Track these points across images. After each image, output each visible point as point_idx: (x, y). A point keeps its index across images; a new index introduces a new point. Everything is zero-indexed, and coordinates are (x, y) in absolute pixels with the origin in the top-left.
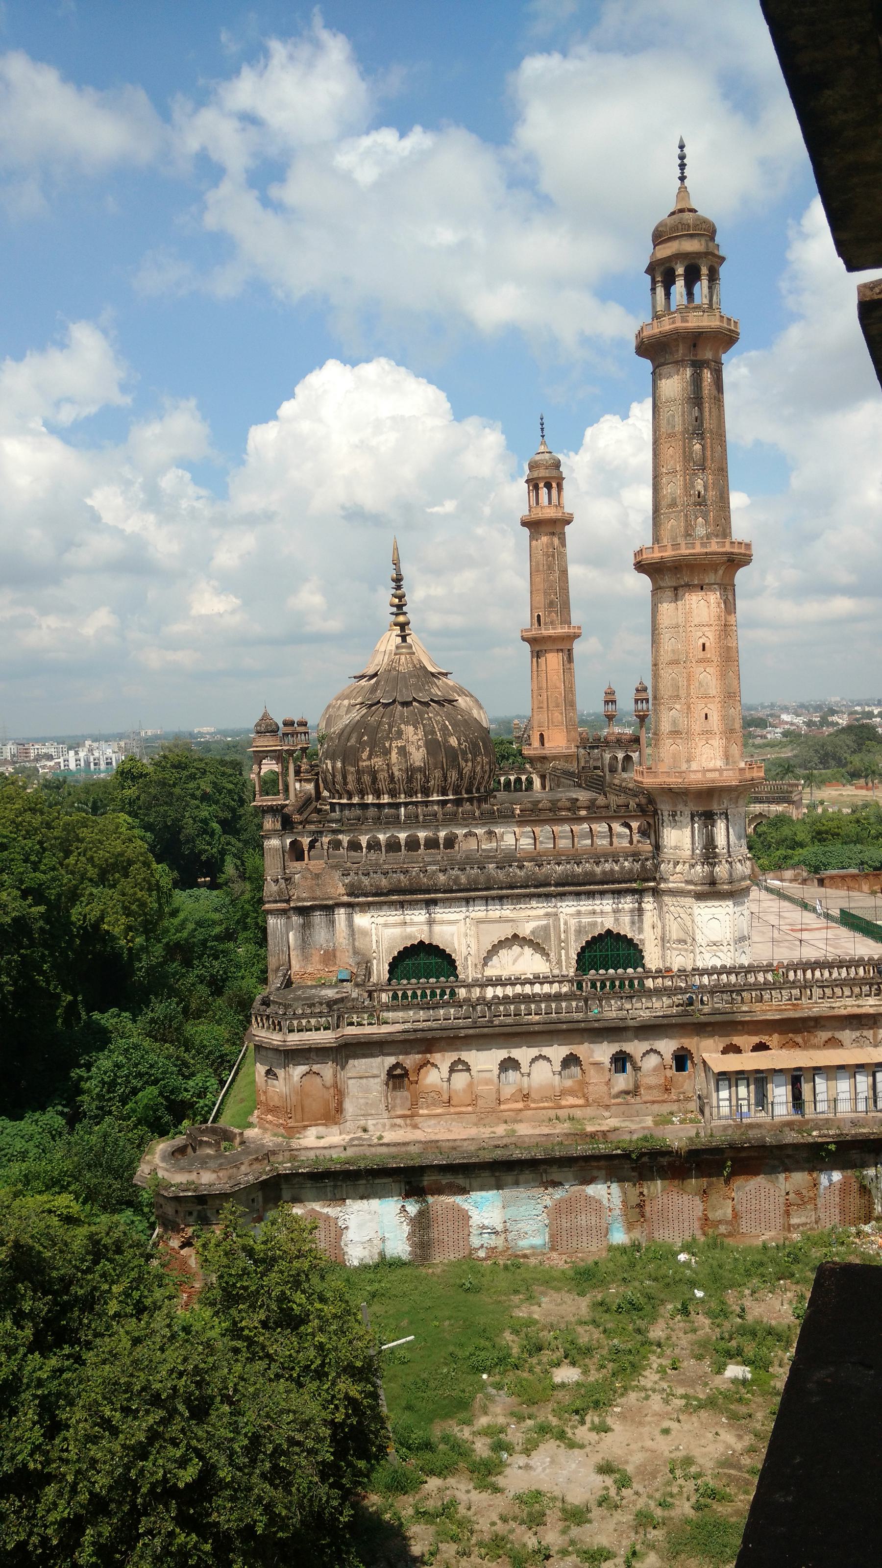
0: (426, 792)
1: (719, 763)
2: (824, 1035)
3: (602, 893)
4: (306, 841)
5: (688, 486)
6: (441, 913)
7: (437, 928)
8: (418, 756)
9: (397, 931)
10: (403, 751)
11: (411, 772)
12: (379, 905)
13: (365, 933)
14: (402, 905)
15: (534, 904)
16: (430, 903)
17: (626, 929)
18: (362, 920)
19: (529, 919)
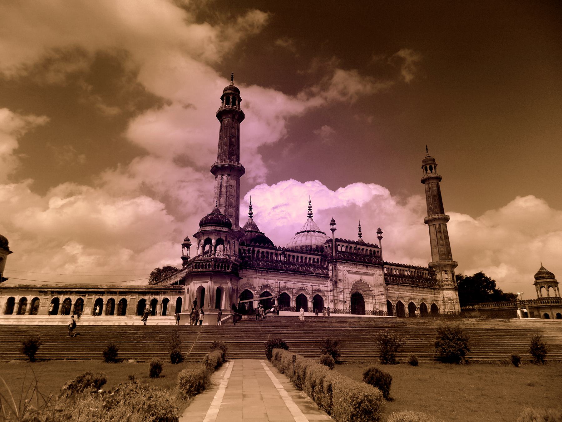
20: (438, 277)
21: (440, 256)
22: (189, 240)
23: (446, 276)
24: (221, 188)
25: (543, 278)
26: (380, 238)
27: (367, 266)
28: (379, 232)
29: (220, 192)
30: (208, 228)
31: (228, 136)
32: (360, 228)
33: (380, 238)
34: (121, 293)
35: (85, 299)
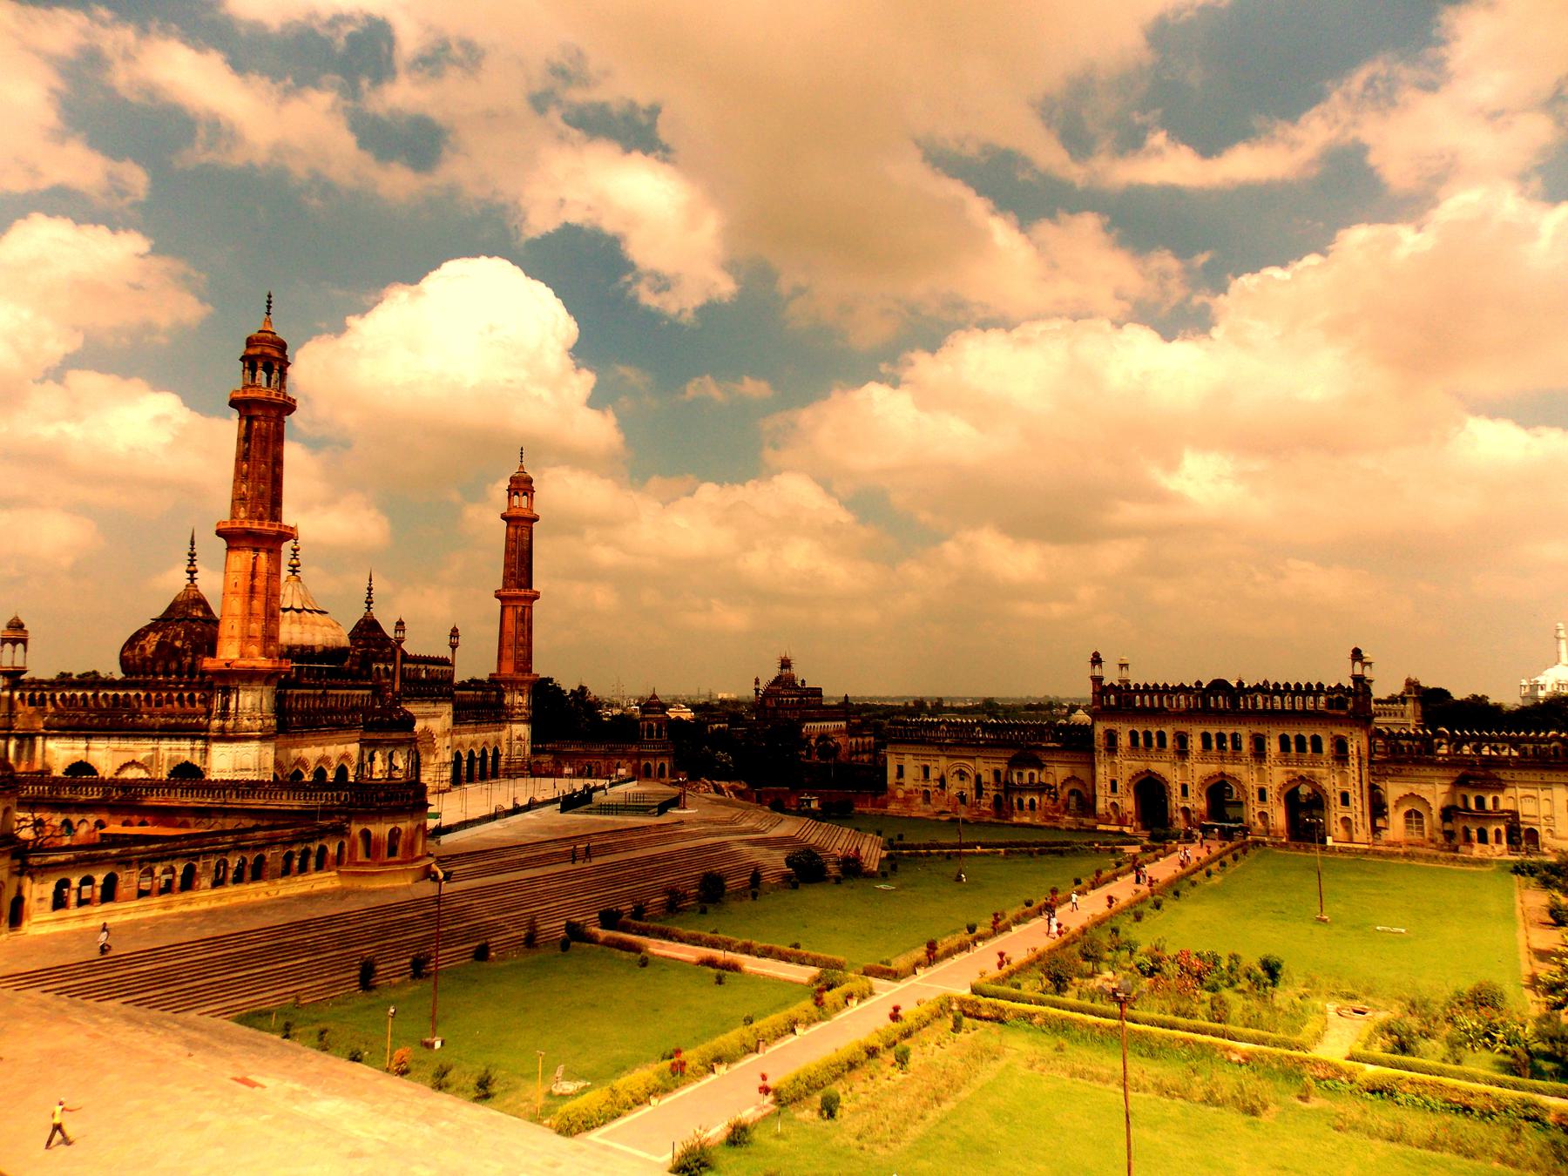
0: (156, 675)
1: (236, 656)
2: (179, 819)
3: (185, 737)
4: (27, 694)
5: (236, 488)
6: (95, 744)
7: (91, 753)
8: (150, 649)
9: (69, 753)
10: (143, 648)
11: (144, 659)
12: (59, 736)
13: (52, 753)
14: (73, 737)
15: (145, 741)
16: (88, 737)
17: (197, 762)
18: (51, 745)
19: (142, 750)
20: (508, 699)
21: (516, 664)
22: (20, 626)
23: (519, 699)
24: (253, 576)
25: (655, 712)
26: (454, 646)
27: (435, 702)
28: (455, 633)
29: (252, 588)
30: (395, 736)
31: (270, 460)
32: (370, 589)
33: (454, 646)
34: (256, 848)
35: (199, 866)
